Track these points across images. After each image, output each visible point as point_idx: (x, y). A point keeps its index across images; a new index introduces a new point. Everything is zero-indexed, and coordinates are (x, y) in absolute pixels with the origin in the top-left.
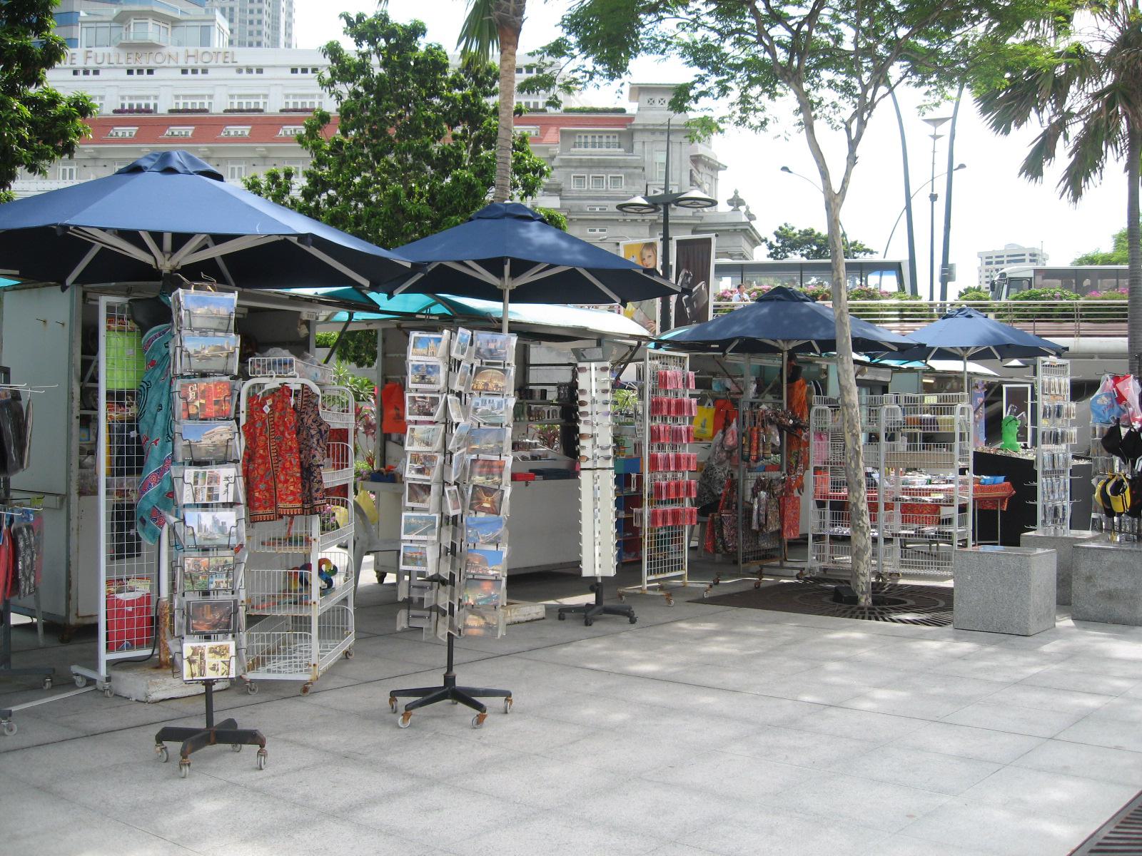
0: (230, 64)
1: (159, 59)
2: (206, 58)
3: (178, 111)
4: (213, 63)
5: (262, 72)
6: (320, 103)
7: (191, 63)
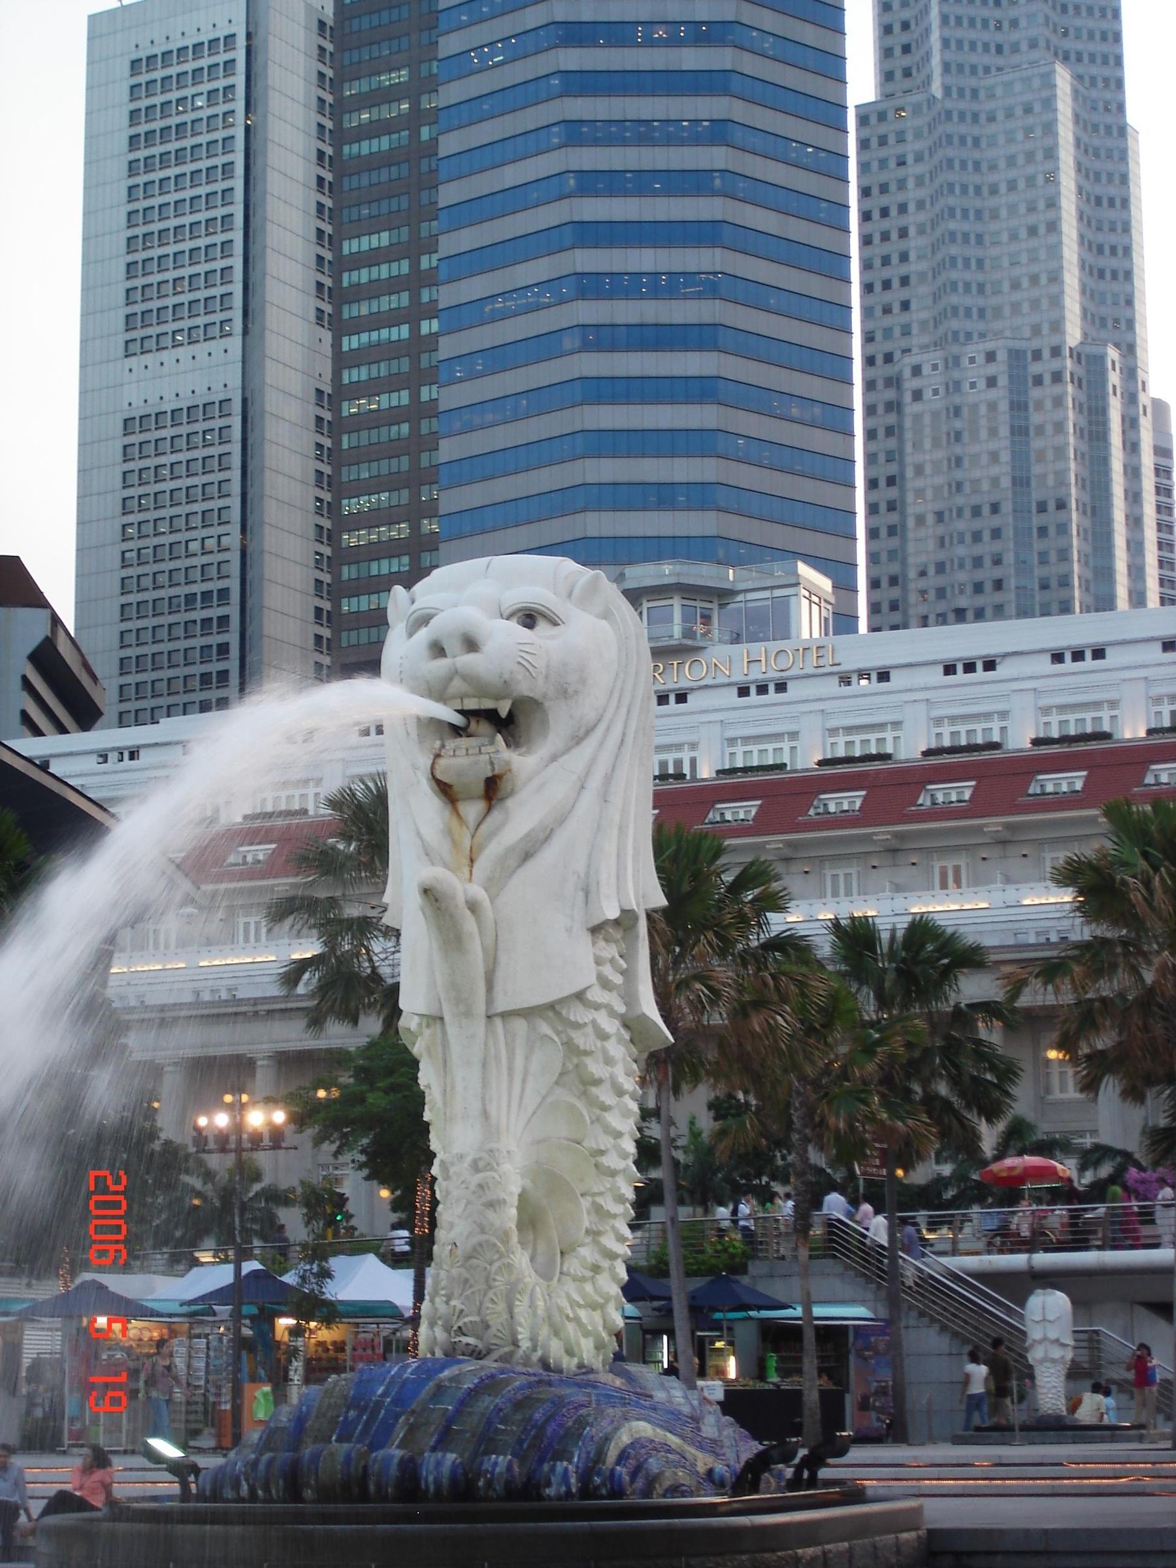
0: (828, 669)
2: (784, 663)
3: (733, 771)
5: (888, 680)
6: (1003, 729)
7: (757, 674)
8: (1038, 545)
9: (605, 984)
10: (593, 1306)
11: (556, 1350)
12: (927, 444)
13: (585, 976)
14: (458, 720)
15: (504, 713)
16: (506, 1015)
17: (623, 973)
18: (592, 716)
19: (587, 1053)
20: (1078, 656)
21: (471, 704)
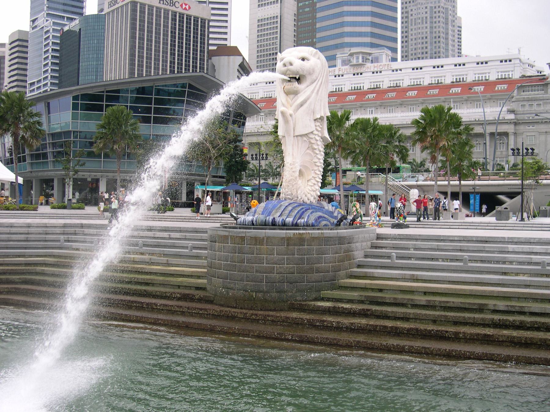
1: (364, 69)
2: (381, 67)
4: (383, 69)
7: (376, 69)
8: (434, 45)
9: (317, 130)
10: (314, 191)
11: (306, 200)
12: (413, 25)
13: (314, 128)
14: (289, 79)
15: (297, 78)
16: (297, 136)
17: (321, 128)
18: (315, 78)
19: (313, 143)
20: (438, 67)
21: (291, 76)
